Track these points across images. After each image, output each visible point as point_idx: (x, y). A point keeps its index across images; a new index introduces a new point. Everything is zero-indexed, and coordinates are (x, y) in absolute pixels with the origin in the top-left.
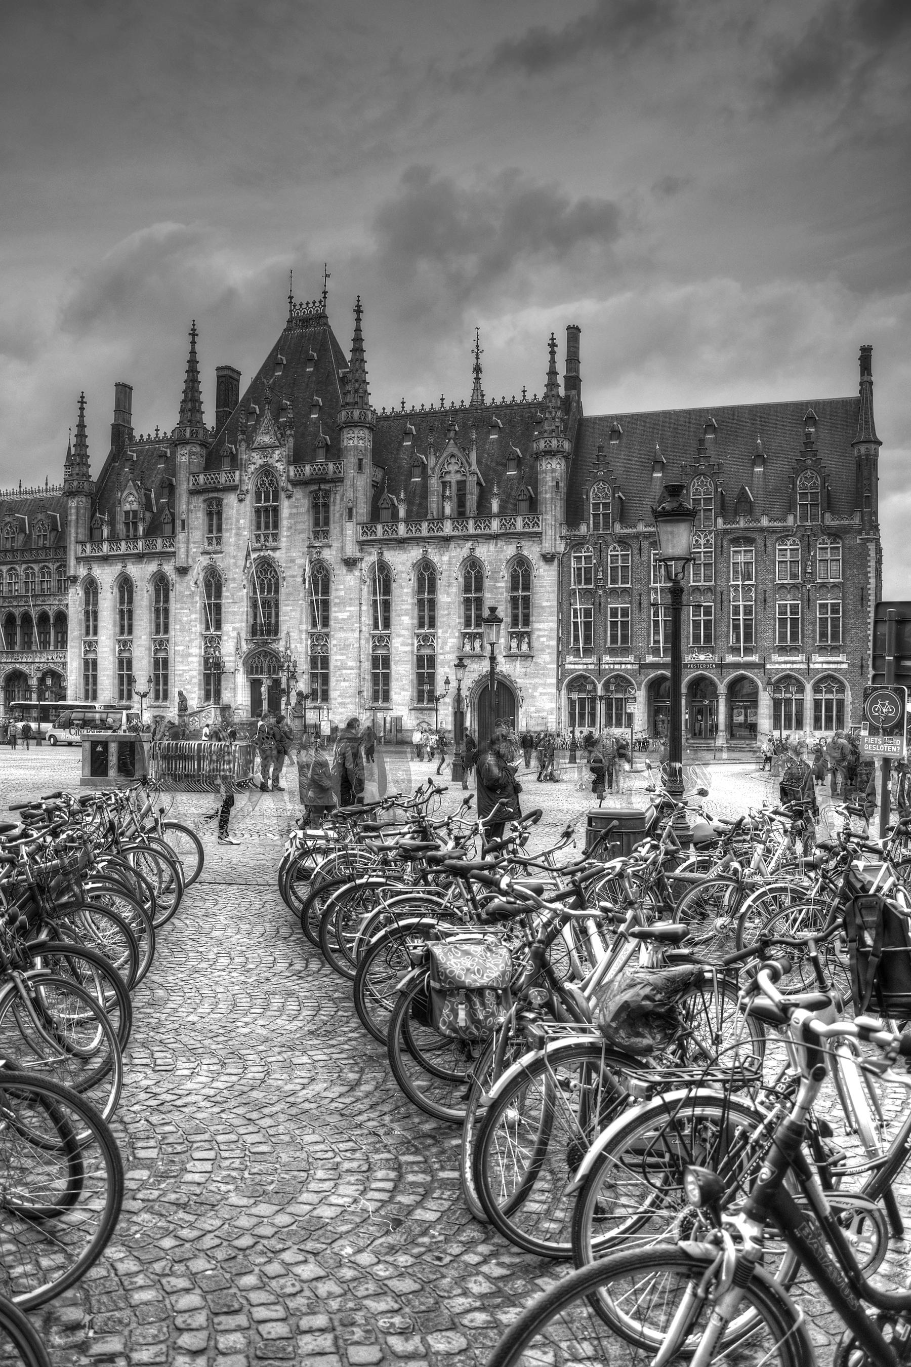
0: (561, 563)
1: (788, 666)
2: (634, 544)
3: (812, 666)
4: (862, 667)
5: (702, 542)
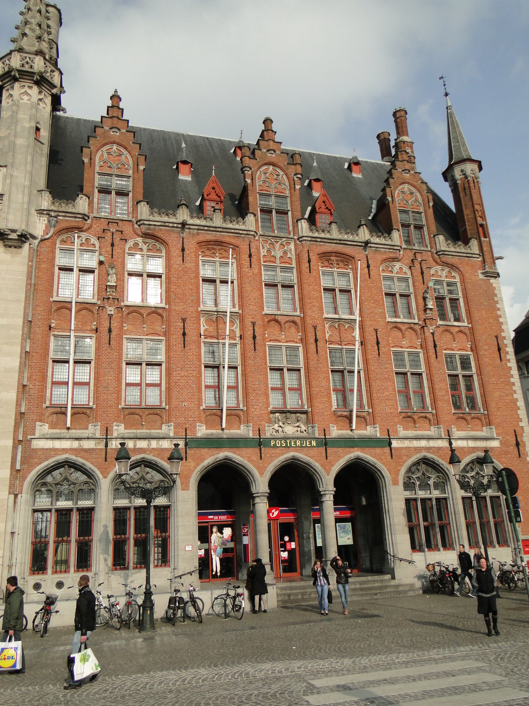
0: (35, 254)
1: (423, 443)
2: (174, 240)
3: (455, 444)
4: (518, 444)
5: (278, 253)
